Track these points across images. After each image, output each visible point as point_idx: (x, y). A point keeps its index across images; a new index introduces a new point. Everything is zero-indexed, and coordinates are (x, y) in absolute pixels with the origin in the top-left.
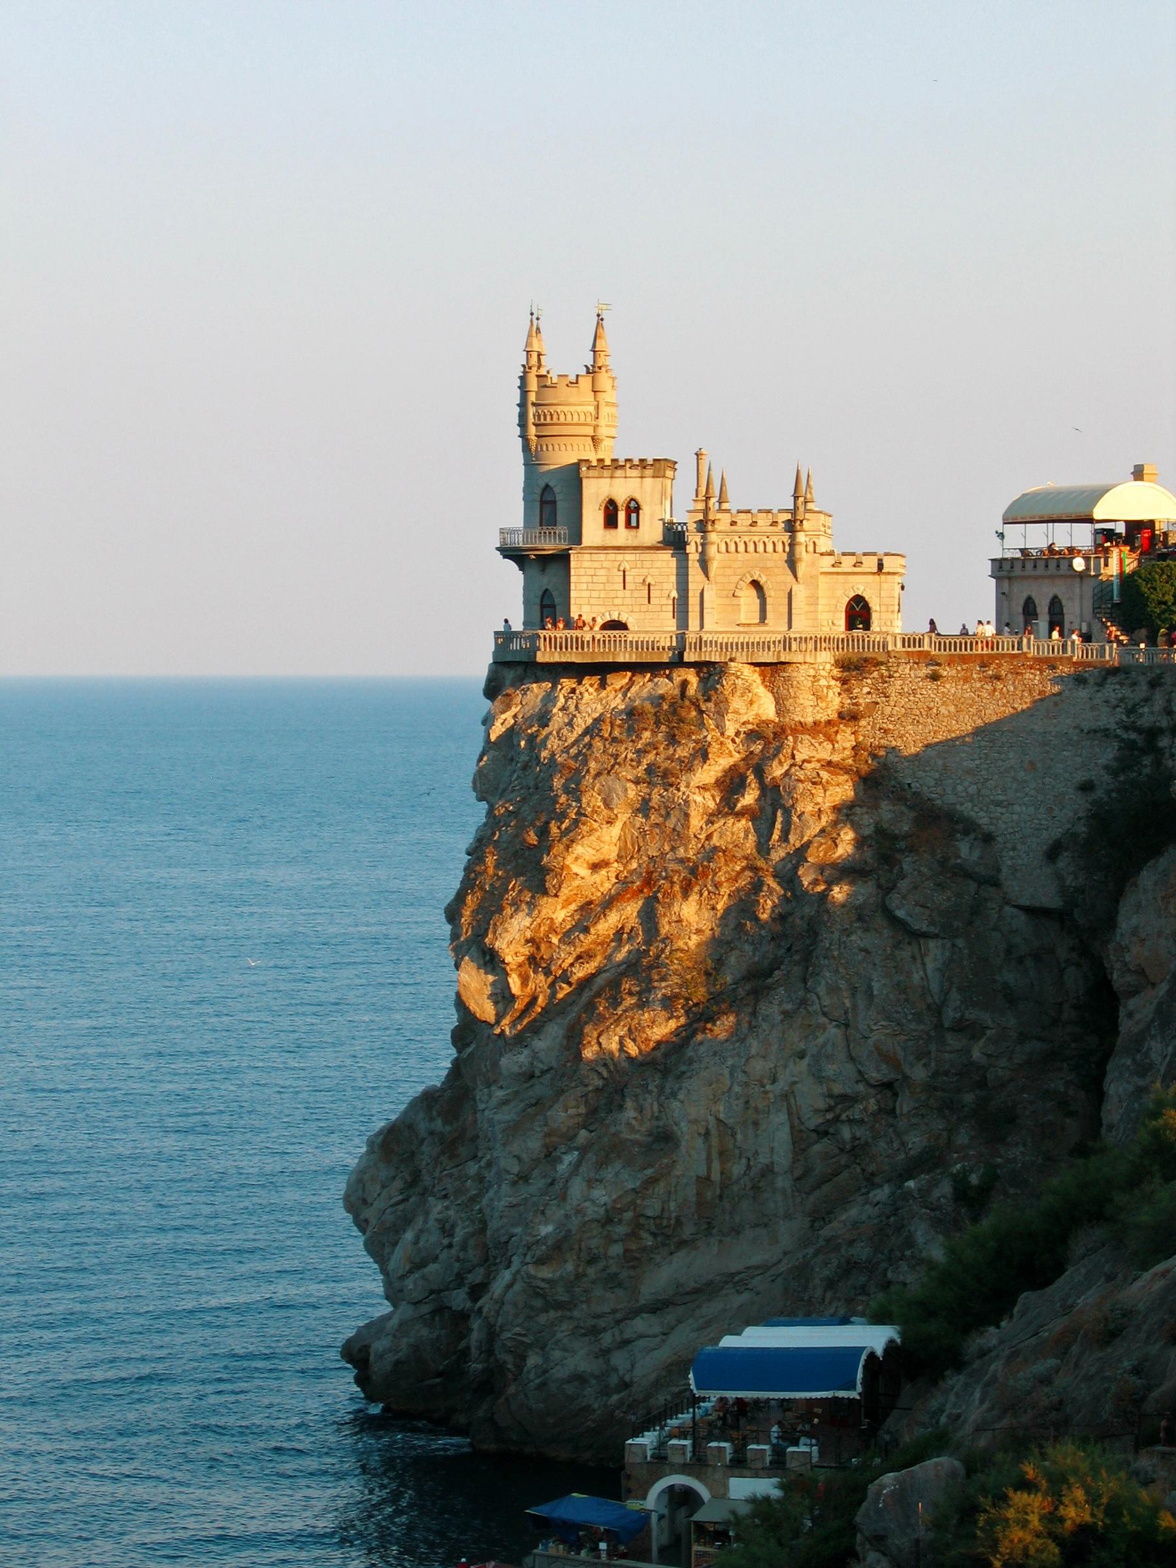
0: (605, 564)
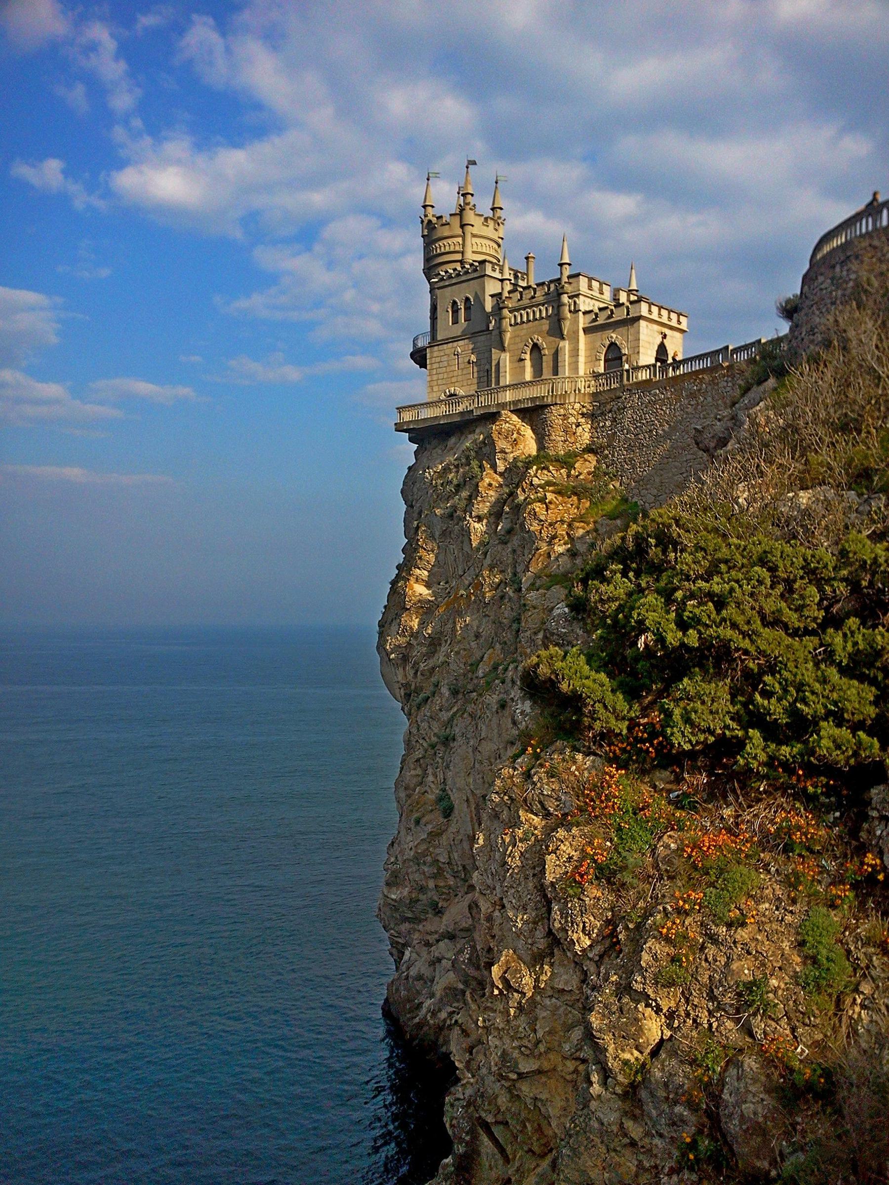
0: (447, 352)
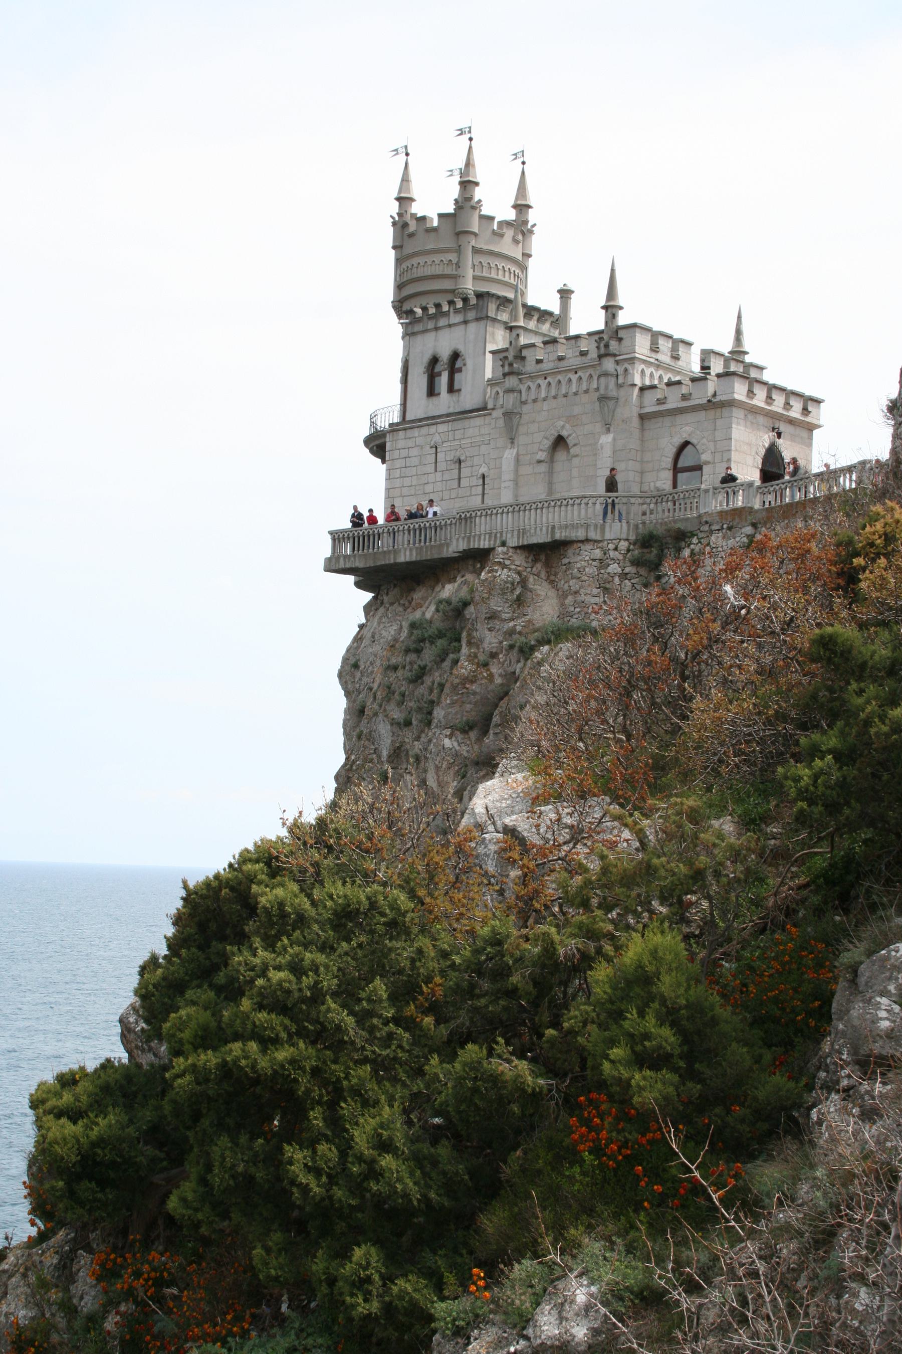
0: (419, 441)
